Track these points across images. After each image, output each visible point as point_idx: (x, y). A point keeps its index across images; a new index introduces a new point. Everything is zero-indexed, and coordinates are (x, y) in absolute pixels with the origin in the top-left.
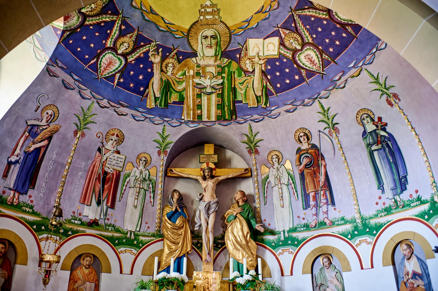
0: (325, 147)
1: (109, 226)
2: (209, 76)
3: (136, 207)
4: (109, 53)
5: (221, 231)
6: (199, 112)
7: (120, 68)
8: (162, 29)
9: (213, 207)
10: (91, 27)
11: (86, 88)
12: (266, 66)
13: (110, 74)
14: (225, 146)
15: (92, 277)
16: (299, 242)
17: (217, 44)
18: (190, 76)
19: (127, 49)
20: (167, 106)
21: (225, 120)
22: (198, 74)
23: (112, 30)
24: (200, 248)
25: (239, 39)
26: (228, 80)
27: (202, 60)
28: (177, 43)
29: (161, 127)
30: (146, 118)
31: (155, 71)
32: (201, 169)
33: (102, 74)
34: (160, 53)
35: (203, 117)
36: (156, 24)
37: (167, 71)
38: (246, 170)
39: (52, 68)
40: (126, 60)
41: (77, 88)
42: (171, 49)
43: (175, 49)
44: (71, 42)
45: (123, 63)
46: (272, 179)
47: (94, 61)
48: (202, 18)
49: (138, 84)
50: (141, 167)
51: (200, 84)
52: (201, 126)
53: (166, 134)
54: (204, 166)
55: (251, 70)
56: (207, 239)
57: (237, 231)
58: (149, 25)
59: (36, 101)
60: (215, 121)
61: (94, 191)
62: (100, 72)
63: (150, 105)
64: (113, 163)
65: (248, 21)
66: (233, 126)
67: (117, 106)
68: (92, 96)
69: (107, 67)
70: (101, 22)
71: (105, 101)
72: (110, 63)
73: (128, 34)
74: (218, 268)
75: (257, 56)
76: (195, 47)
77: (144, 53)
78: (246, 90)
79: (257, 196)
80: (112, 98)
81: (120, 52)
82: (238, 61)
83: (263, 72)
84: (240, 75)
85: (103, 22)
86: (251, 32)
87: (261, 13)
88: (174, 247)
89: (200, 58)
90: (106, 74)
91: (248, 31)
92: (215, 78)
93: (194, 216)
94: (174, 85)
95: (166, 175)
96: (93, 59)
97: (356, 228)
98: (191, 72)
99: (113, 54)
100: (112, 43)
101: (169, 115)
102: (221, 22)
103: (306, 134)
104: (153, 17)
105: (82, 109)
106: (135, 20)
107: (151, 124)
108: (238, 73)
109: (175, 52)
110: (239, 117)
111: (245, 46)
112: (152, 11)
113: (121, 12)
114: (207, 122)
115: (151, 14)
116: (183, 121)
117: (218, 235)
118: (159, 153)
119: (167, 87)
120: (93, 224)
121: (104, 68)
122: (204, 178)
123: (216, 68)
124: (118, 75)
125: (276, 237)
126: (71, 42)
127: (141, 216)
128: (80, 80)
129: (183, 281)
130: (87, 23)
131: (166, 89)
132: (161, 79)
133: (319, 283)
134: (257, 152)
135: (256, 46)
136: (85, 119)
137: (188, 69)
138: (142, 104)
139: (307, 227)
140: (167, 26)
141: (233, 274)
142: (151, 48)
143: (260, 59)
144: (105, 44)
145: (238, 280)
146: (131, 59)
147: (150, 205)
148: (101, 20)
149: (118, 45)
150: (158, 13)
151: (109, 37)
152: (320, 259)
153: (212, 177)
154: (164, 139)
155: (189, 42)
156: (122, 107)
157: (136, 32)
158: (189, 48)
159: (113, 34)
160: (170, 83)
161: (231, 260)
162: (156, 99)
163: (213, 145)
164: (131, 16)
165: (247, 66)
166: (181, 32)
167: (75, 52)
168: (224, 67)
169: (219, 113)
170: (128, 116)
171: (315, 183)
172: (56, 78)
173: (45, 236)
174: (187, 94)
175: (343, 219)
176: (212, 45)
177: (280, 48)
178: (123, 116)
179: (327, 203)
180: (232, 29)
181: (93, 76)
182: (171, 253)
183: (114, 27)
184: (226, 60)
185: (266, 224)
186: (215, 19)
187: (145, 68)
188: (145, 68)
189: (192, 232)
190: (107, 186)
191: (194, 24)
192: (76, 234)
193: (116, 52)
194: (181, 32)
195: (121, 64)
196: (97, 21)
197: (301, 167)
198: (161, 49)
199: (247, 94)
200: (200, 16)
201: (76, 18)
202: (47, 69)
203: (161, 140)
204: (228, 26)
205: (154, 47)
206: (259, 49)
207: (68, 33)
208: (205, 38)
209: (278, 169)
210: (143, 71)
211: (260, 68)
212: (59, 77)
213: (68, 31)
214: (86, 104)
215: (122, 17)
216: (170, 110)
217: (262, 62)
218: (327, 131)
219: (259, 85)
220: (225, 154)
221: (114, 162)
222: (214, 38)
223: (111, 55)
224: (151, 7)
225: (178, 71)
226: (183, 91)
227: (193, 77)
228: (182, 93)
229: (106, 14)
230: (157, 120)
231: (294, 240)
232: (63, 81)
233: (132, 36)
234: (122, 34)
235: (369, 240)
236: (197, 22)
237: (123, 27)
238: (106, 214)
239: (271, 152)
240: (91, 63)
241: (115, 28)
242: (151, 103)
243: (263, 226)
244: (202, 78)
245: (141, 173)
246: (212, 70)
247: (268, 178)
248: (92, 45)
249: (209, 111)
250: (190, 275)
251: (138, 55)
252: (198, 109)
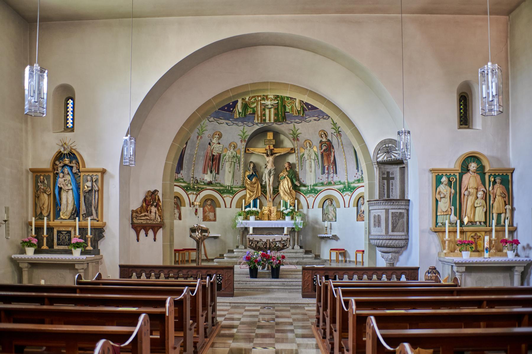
0: (335, 142)
1: (218, 183)
3: (230, 172)
5: (277, 185)
9: (273, 172)
15: (212, 209)
16: (318, 192)
21: (279, 122)
24: (266, 193)
29: (242, 127)
32: (266, 150)
38: (292, 149)
46: (306, 156)
50: (232, 150)
52: (265, 125)
53: (245, 131)
54: (268, 148)
56: (270, 189)
57: (285, 185)
61: (208, 166)
64: (217, 149)
74: (275, 204)
79: (297, 165)
88: (252, 194)
93: (262, 176)
95: (245, 151)
97: (345, 187)
103: (325, 134)
117: (276, 186)
118: (241, 141)
119: (245, 106)
120: (210, 183)
122: (268, 156)
125: (306, 188)
127: (233, 177)
129: (258, 212)
132: (242, 103)
133: (326, 212)
134: (298, 140)
136: (202, 129)
138: (232, 116)
139: (323, 184)
141: (282, 208)
145: (284, 212)
147: (237, 171)
152: (327, 201)
153: (272, 155)
154: (244, 133)
161: (282, 201)
162: (239, 113)
171: (329, 161)
173: (190, 192)
175: (340, 182)
179: (333, 173)
182: (251, 197)
185: (302, 181)
189: (261, 185)
190: (214, 162)
192: (203, 189)
197: (322, 151)
203: (242, 134)
209: (309, 151)
218: (335, 134)
221: (217, 149)
227: (261, 100)
231: (315, 190)
235: (350, 194)
238: (215, 178)
239: (306, 140)
242: (237, 115)
243: (300, 183)
245: (232, 153)
247: (304, 154)
250: (261, 208)
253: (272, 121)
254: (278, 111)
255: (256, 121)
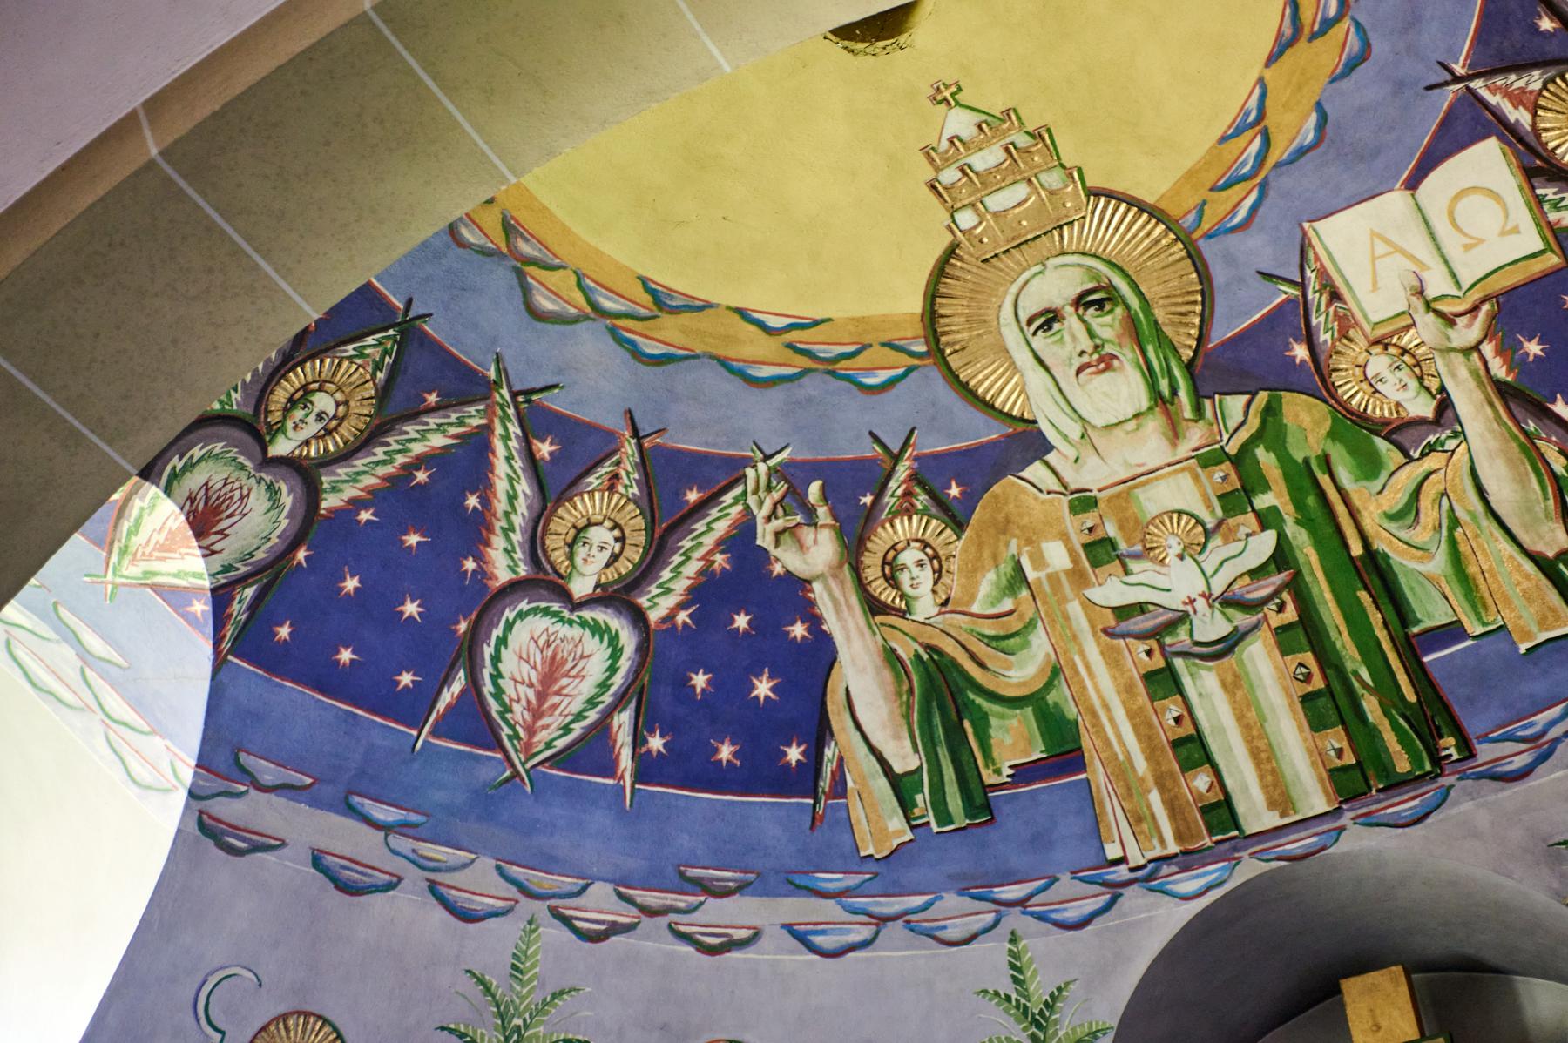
2: (1173, 541)
4: (521, 615)
6: (1202, 781)
7: (618, 680)
8: (766, 372)
10: (365, 516)
11: (464, 856)
12: (1508, 350)
13: (578, 729)
14: (1491, 956)
17: (1133, 331)
18: (1053, 579)
19: (615, 558)
20: (987, 807)
21: (1396, 784)
22: (1100, 551)
23: (489, 486)
25: (1258, 249)
26: (1304, 521)
27: (1092, 460)
28: (890, 418)
29: (993, 951)
30: (882, 920)
31: (832, 624)
33: (528, 745)
34: (823, 512)
35: (1241, 808)
36: (723, 362)
37: (903, 596)
39: (226, 809)
40: (638, 617)
41: (413, 876)
42: (873, 460)
43: (896, 459)
44: (284, 632)
45: (629, 640)
47: (457, 686)
48: (966, 219)
49: (761, 731)
51: (1141, 608)
52: (1249, 868)
53: (1039, 990)
55: (1424, 408)
58: (683, 377)
59: (191, 1019)
60: (1335, 813)
62: (516, 736)
63: (880, 834)
65: (1255, 122)
66: (1468, 806)
67: (682, 901)
68: (513, 892)
69: (542, 697)
70: (404, 467)
71: (601, 893)
72: (555, 667)
73: (589, 471)
75: (1418, 304)
76: (1009, 401)
77: (724, 544)
78: (1453, 543)
80: (634, 864)
81: (581, 587)
82: (1318, 381)
83: (1502, 388)
84: (1370, 466)
85: (420, 462)
86: (1303, 180)
87: (1302, 44)
89: (1071, 453)
90: (552, 735)
91: (1284, 182)
92: (1216, 541)
94: (981, 665)
96: (446, 681)
98: (1057, 556)
99: (546, 612)
100: (519, 555)
101: (1017, 861)
102: (1096, 193)
104: (685, 331)
105: (481, 981)
106: (594, 384)
107: (928, 952)
108: (1353, 451)
109: (903, 471)
110: (1484, 738)
111: (1311, 275)
112: (662, 301)
113: (492, 374)
114: (1277, 831)
115: (667, 320)
116: (1122, 872)
119: (944, 696)
121: (529, 707)
123: (1196, 478)
124: (623, 721)
126: (284, 632)
128: (414, 818)
130: (330, 502)
131: (942, 708)
132: (891, 657)
135: (1381, 249)
137: (1029, 542)
140: (790, 346)
142: (755, 498)
143: (1450, 320)
144: (482, 574)
146: (660, 603)
148: (401, 459)
149: (559, 556)
150: (704, 294)
151: (490, 530)
155: (965, 385)
156: (711, 900)
157: (630, 448)
158: (978, 417)
159: (501, 505)
160: (954, 662)
163: (1397, 970)
164: (560, 371)
165: (1389, 389)
166: (888, 344)
167: (328, 681)
168: (1246, 448)
169: (1340, 753)
170: (764, 942)
172: (269, 857)
174: (1080, 697)
176: (1108, 349)
177: (1540, 201)
178: (735, 955)
180: (1181, 207)
181: (485, 774)
183: (490, 467)
184: (1235, 404)
186: (1051, 193)
187: (768, 627)
188: (768, 627)
191: (941, 270)
193: (564, 595)
194: (888, 344)
195: (616, 654)
196: (382, 471)
198: (814, 490)
199: (1472, 569)
200: (953, 212)
201: (258, 501)
202: (201, 825)
204: (1150, 199)
205: (769, 488)
206: (1412, 258)
207: (250, 592)
208: (1047, 326)
210: (765, 647)
211: (1474, 373)
212: (283, 844)
213: (243, 581)
214: (492, 944)
215: (514, 395)
216: (1012, 823)
217: (1468, 332)
219: (1523, 483)
220: (1516, 1009)
222: (1100, 304)
223: (540, 624)
224: (645, 282)
225: (973, 572)
226: (1049, 686)
227: (1078, 578)
228: (1051, 698)
229: (414, 416)
230: (957, 911)
232: (317, 859)
233: (616, 476)
234: (553, 488)
236: (951, 252)
237: (544, 449)
240: (441, 706)
241: (501, 468)
242: (878, 823)
244: (1133, 565)
246: (1181, 493)
248: (411, 608)
249: (1264, 756)
251: (693, 568)
252: (1188, 766)
253: (1316, 801)
254: (1328, 659)
255: (1122, 843)
